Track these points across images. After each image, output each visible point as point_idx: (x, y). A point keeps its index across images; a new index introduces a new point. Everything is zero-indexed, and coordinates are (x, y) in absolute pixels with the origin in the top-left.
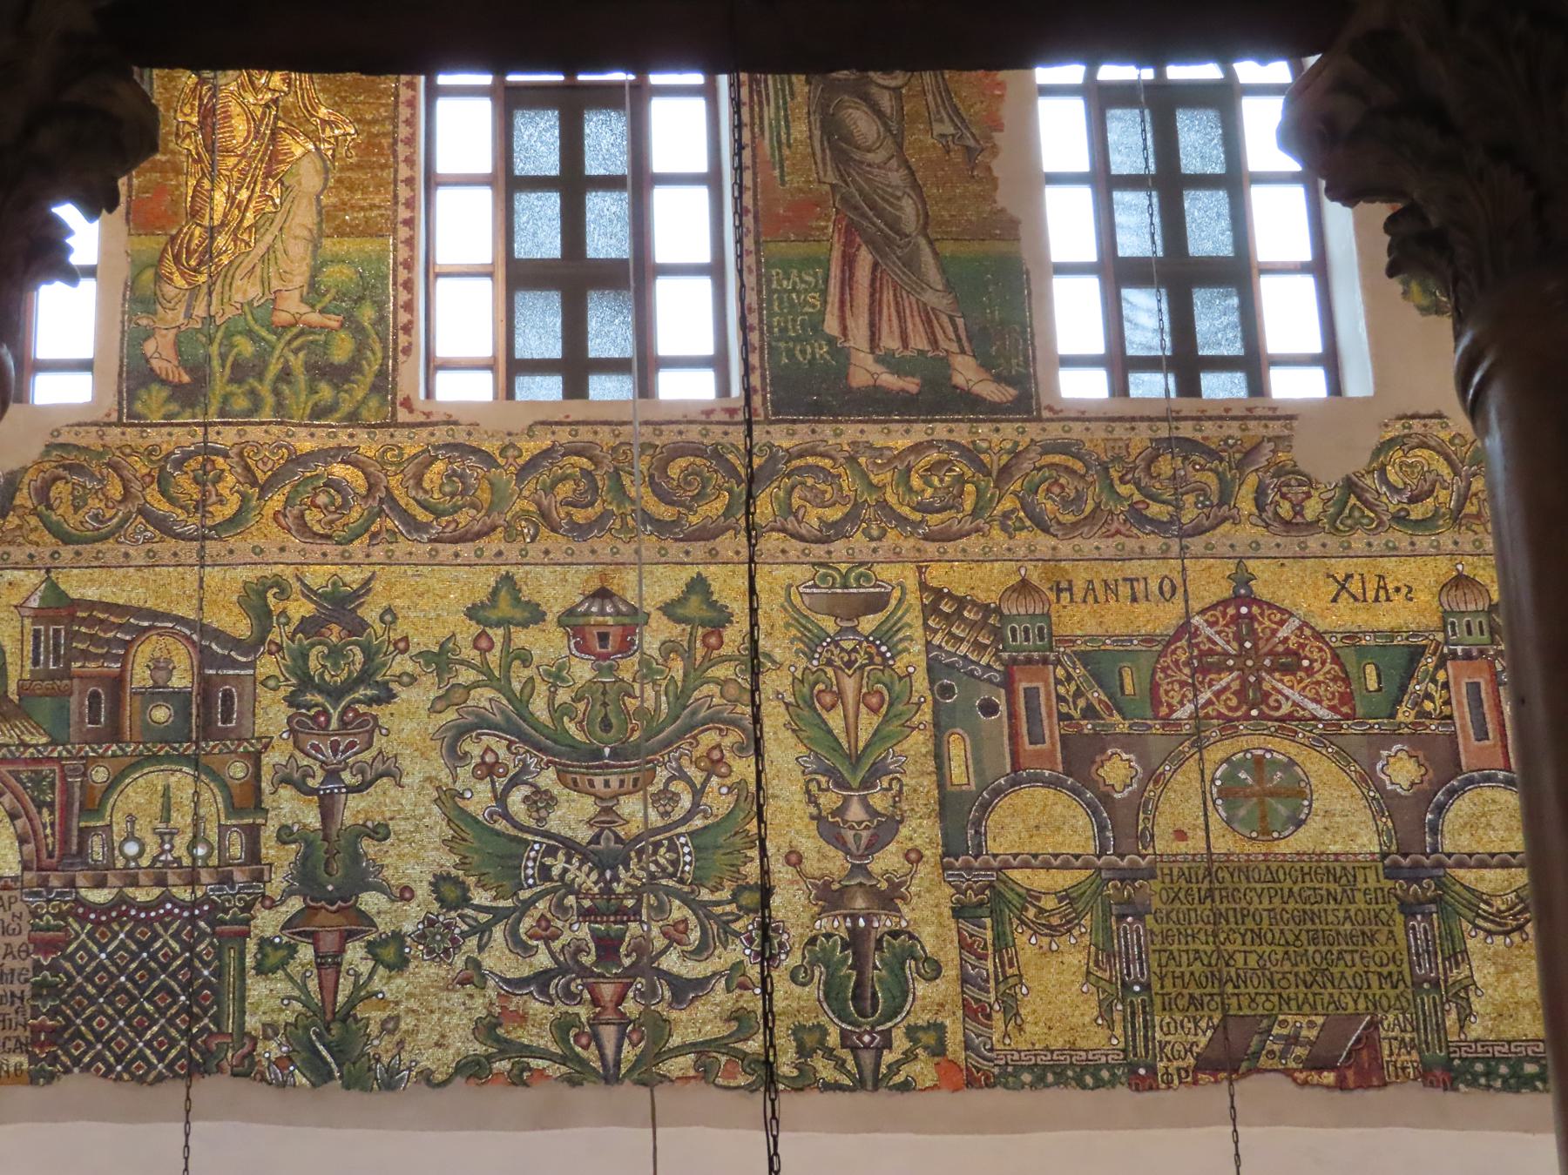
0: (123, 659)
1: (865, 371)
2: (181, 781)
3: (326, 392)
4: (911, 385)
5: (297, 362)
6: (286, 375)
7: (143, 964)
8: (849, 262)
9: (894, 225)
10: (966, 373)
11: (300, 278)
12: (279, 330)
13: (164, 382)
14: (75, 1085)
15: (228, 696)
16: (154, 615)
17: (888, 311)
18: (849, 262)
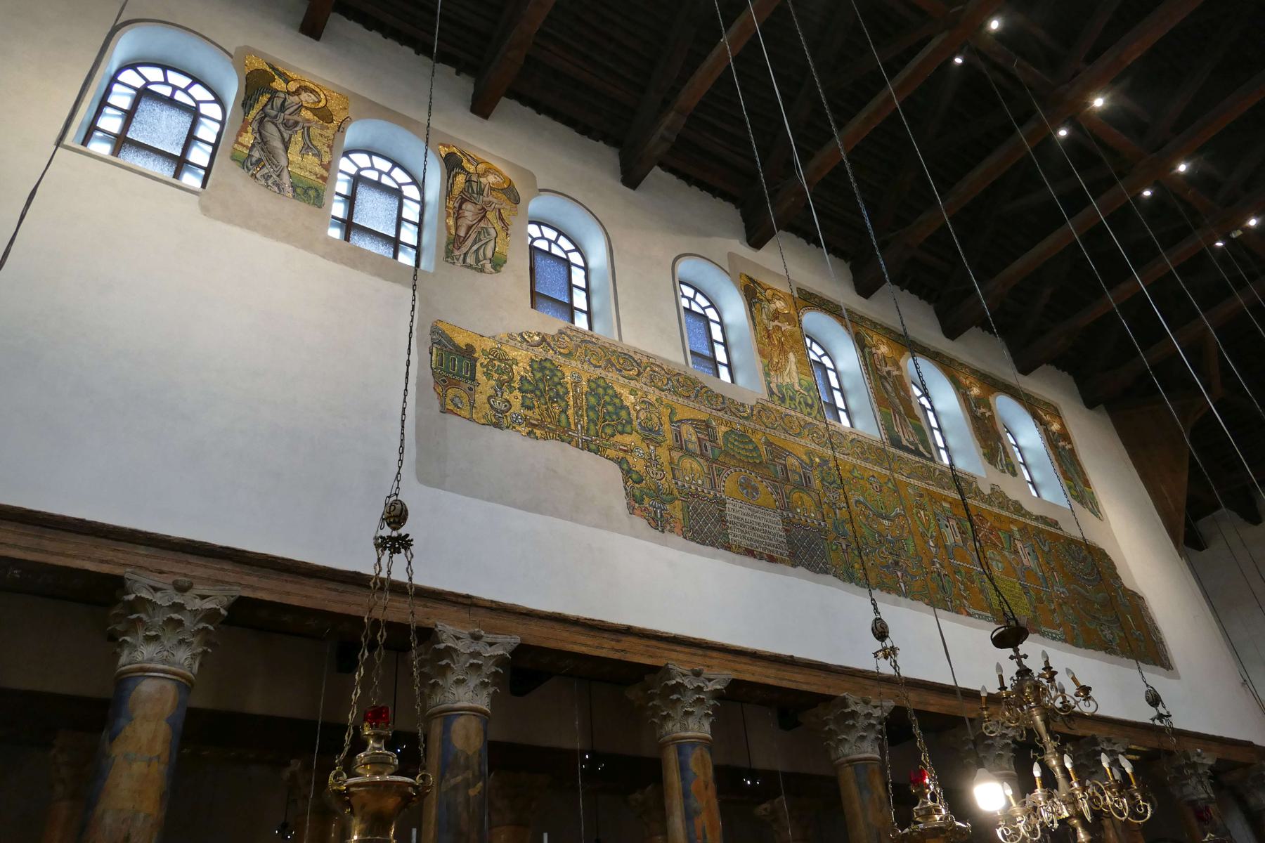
0: (785, 460)
1: (905, 442)
2: (805, 497)
3: (809, 410)
4: (913, 448)
5: (802, 400)
6: (800, 403)
7: (808, 541)
8: (895, 416)
9: (900, 411)
10: (921, 448)
11: (797, 381)
12: (797, 391)
13: (776, 395)
14: (801, 569)
15: (809, 477)
16: (790, 452)
17: (905, 430)
18: (895, 416)
